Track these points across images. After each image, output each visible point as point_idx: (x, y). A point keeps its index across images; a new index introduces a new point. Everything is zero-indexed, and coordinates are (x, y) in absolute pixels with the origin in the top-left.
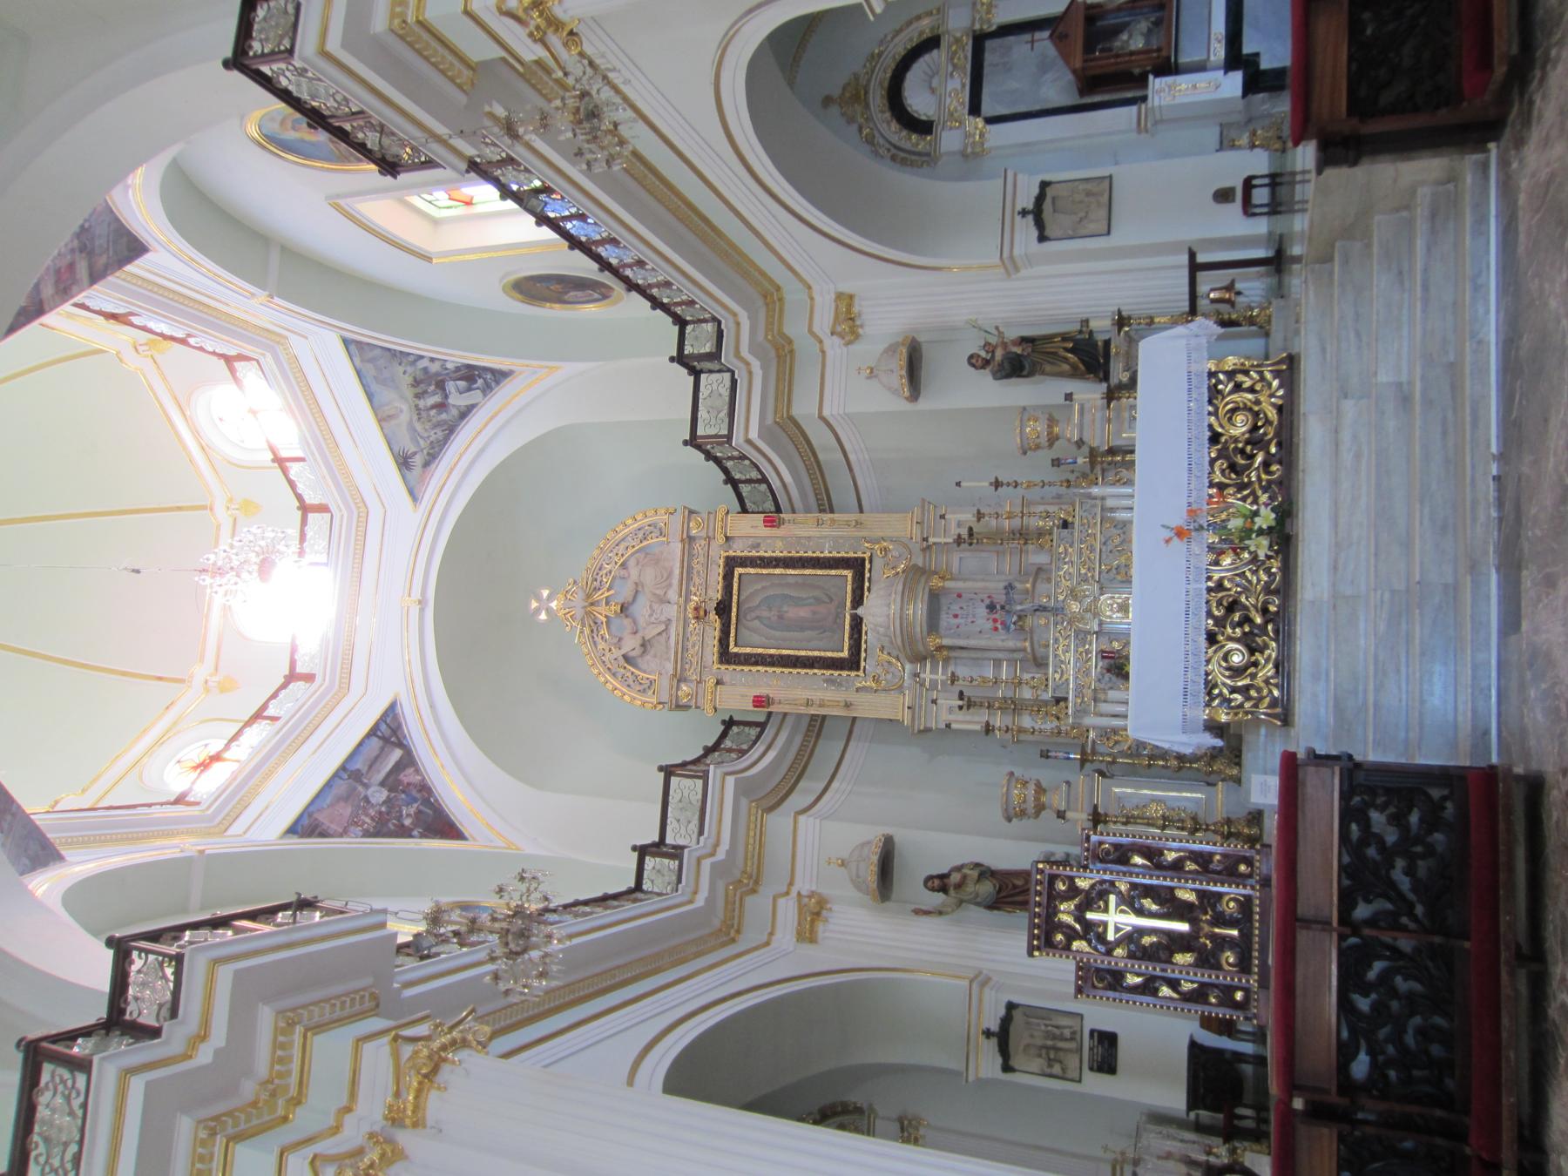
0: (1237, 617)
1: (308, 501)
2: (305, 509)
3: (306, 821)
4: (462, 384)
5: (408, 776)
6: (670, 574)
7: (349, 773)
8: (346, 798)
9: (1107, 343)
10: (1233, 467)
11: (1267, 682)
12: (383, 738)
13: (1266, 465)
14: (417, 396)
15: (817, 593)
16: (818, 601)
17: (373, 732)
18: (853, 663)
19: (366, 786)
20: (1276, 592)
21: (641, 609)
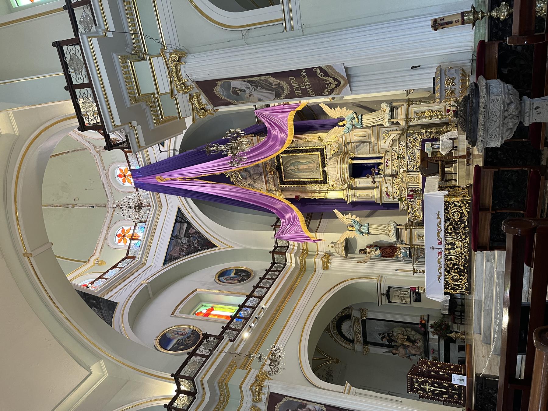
0: (456, 267)
3: (168, 257)
5: (191, 231)
7: (174, 237)
8: (176, 245)
10: (454, 228)
11: (465, 284)
13: (464, 228)
15: (309, 160)
16: (310, 163)
17: (176, 221)
18: (325, 181)
19: (180, 239)
20: (467, 262)
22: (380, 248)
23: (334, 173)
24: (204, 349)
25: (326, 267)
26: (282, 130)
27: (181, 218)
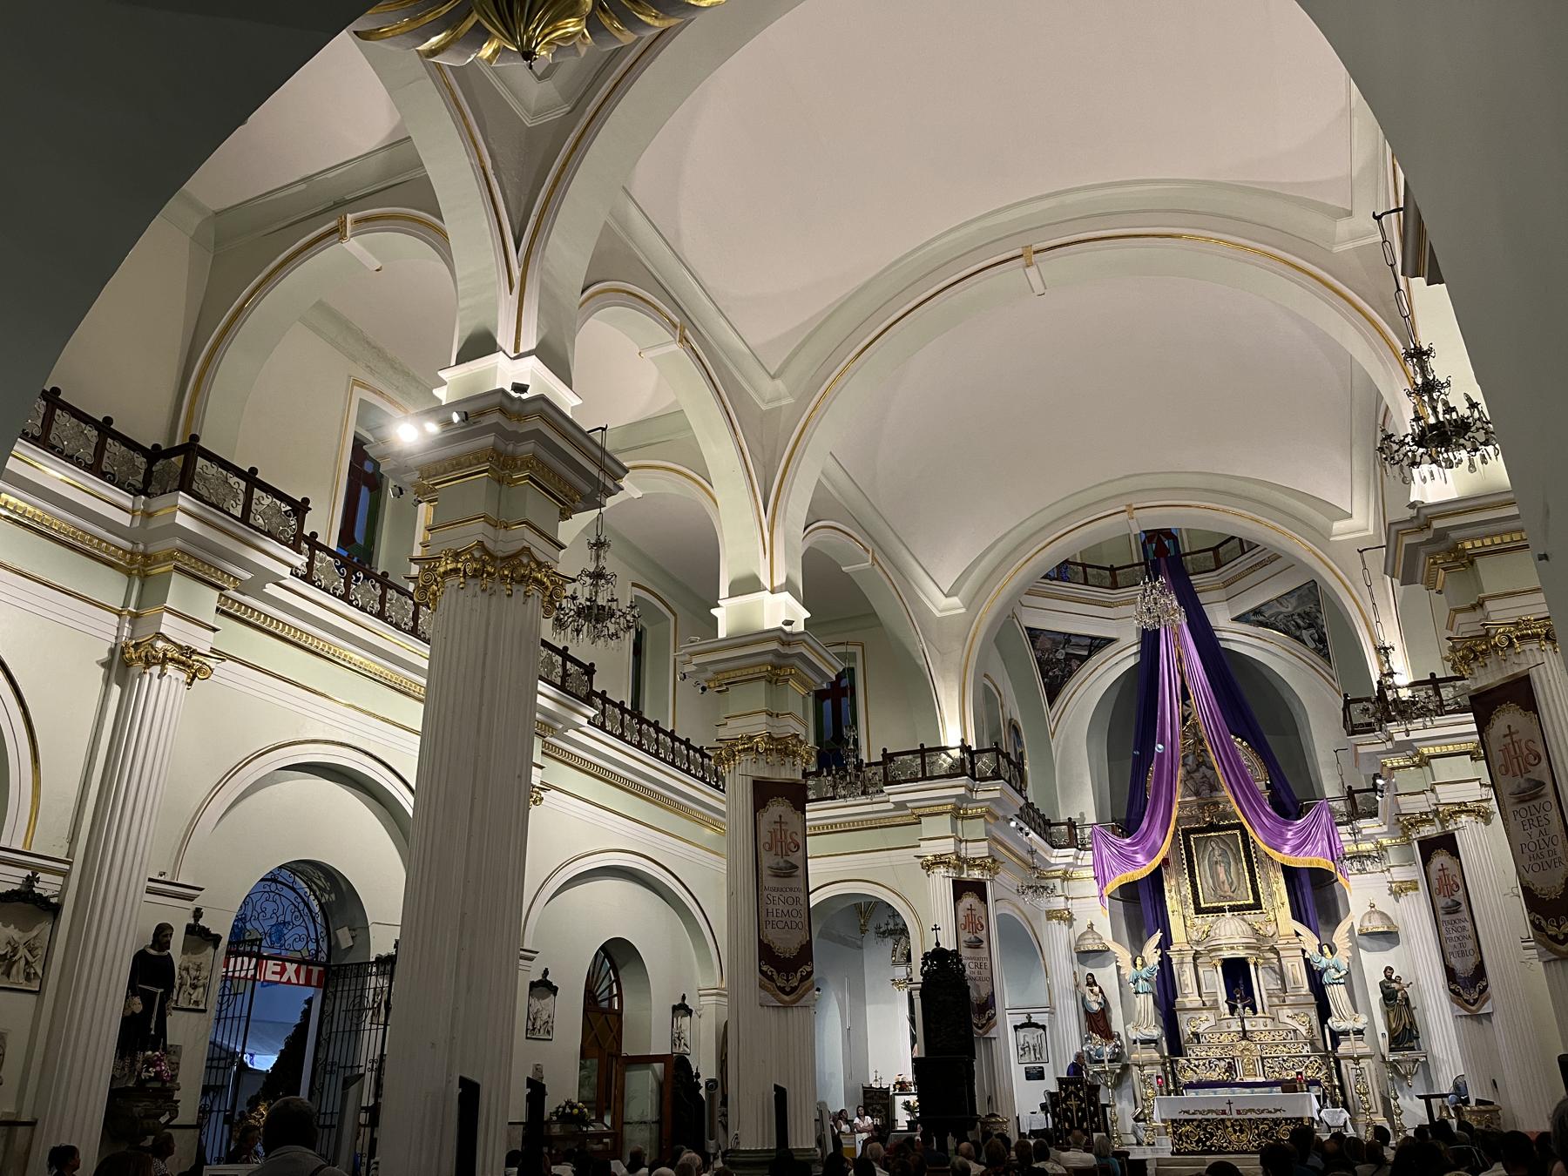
7: (1068, 637)
9: (1412, 1049)
16: (1231, 884)
17: (1093, 638)
18: (1199, 910)
25: (1051, 915)
26: (1296, 848)
27: (1097, 644)
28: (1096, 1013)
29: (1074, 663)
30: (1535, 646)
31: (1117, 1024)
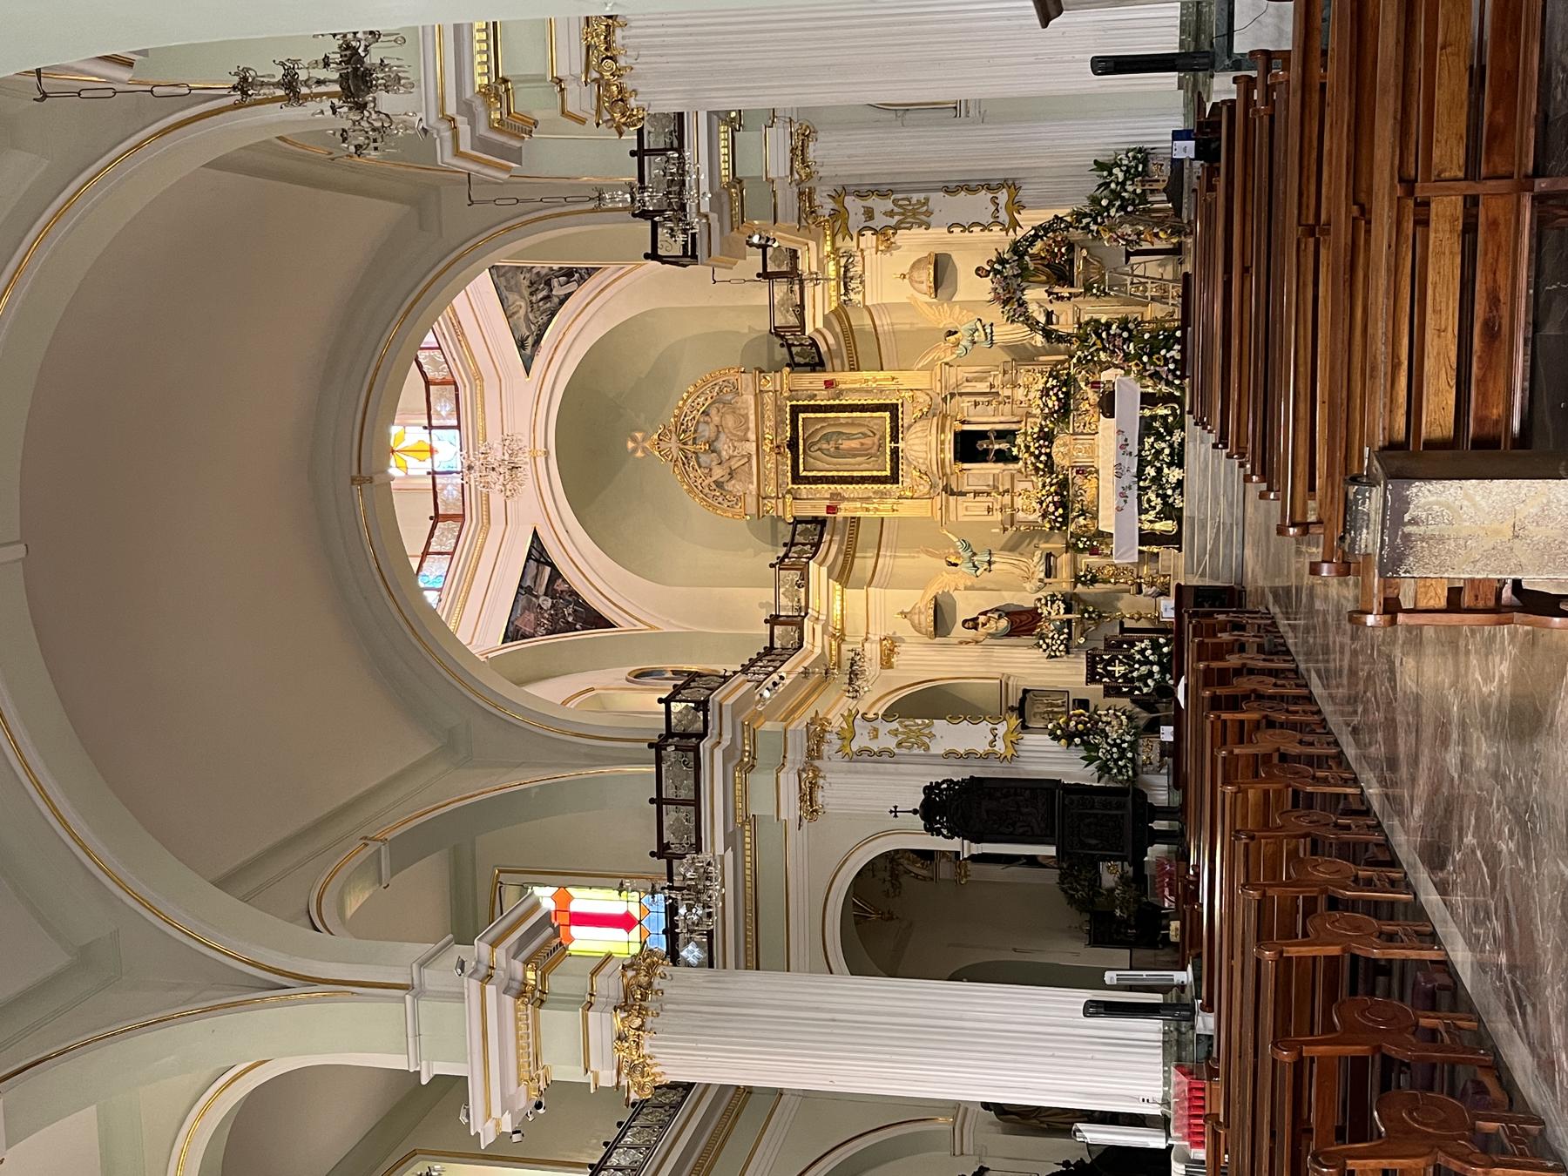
1: (430, 375)
2: (428, 383)
4: (563, 279)
5: (559, 586)
6: (746, 417)
7: (524, 590)
8: (527, 608)
12: (537, 560)
14: (531, 294)
18: (894, 478)
19: (537, 597)
21: (724, 447)
22: (1007, 614)
23: (924, 448)
24: (553, 897)
25: (886, 663)
28: (1012, 623)
29: (559, 586)
30: (618, 32)
31: (1026, 599)
